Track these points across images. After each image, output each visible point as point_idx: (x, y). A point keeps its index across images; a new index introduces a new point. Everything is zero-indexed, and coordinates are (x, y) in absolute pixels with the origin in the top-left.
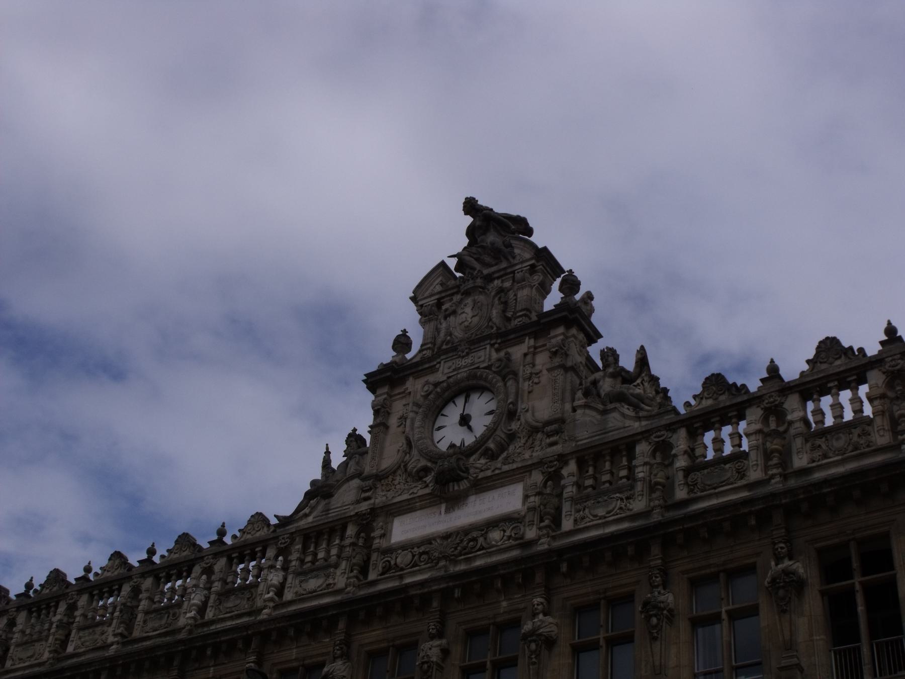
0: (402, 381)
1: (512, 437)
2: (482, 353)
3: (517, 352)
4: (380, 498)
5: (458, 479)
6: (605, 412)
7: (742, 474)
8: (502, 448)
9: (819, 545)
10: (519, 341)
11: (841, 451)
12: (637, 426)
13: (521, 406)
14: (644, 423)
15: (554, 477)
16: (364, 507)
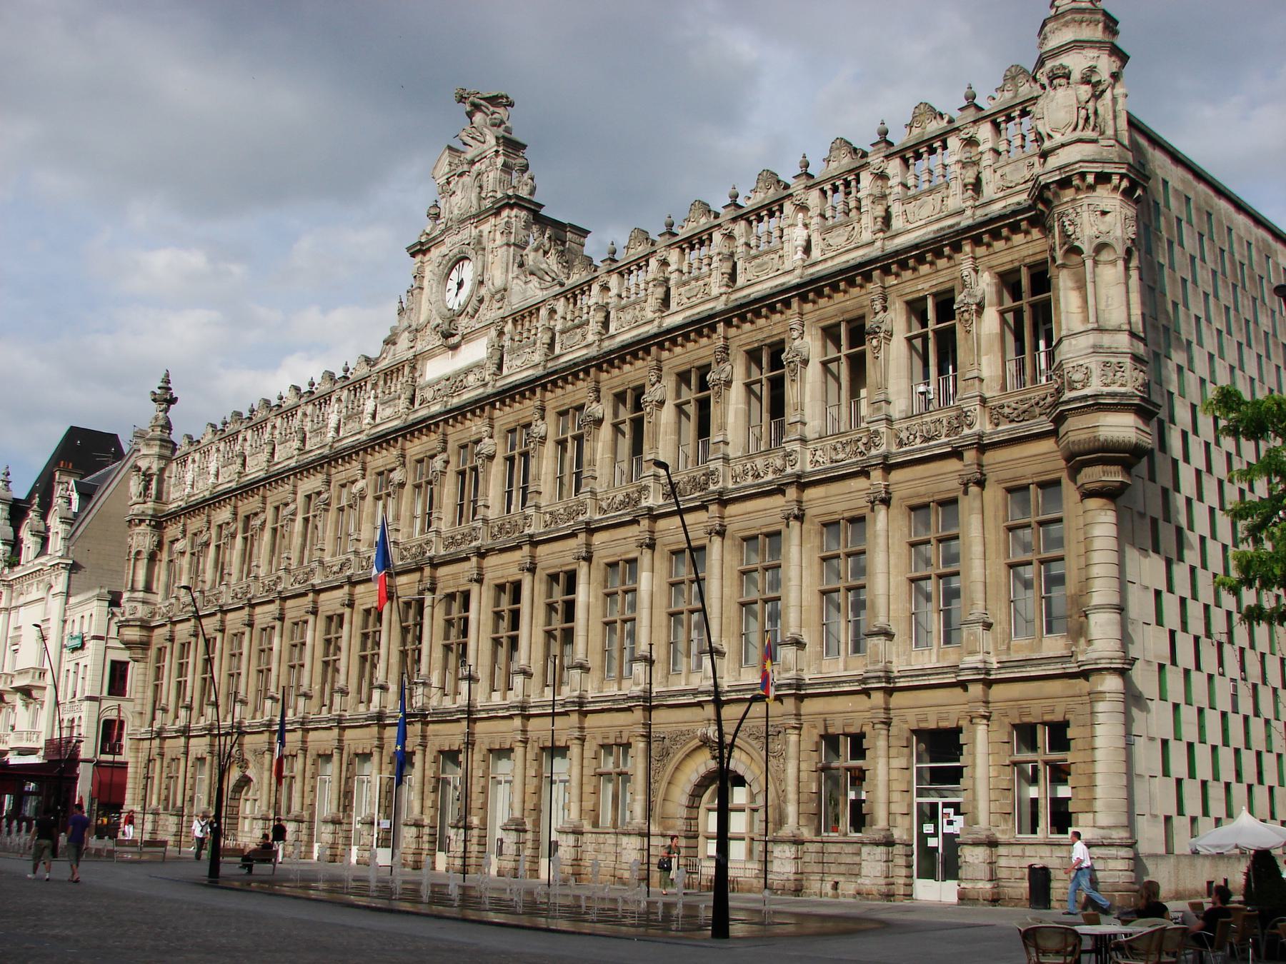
0: (428, 250)
1: (481, 301)
2: (466, 231)
3: (486, 228)
4: (419, 347)
5: (453, 335)
6: (526, 283)
7: (584, 337)
8: (476, 311)
9: (614, 391)
10: (485, 220)
11: (629, 323)
12: (540, 295)
13: (486, 277)
14: (545, 292)
15: (501, 333)
16: (410, 354)
